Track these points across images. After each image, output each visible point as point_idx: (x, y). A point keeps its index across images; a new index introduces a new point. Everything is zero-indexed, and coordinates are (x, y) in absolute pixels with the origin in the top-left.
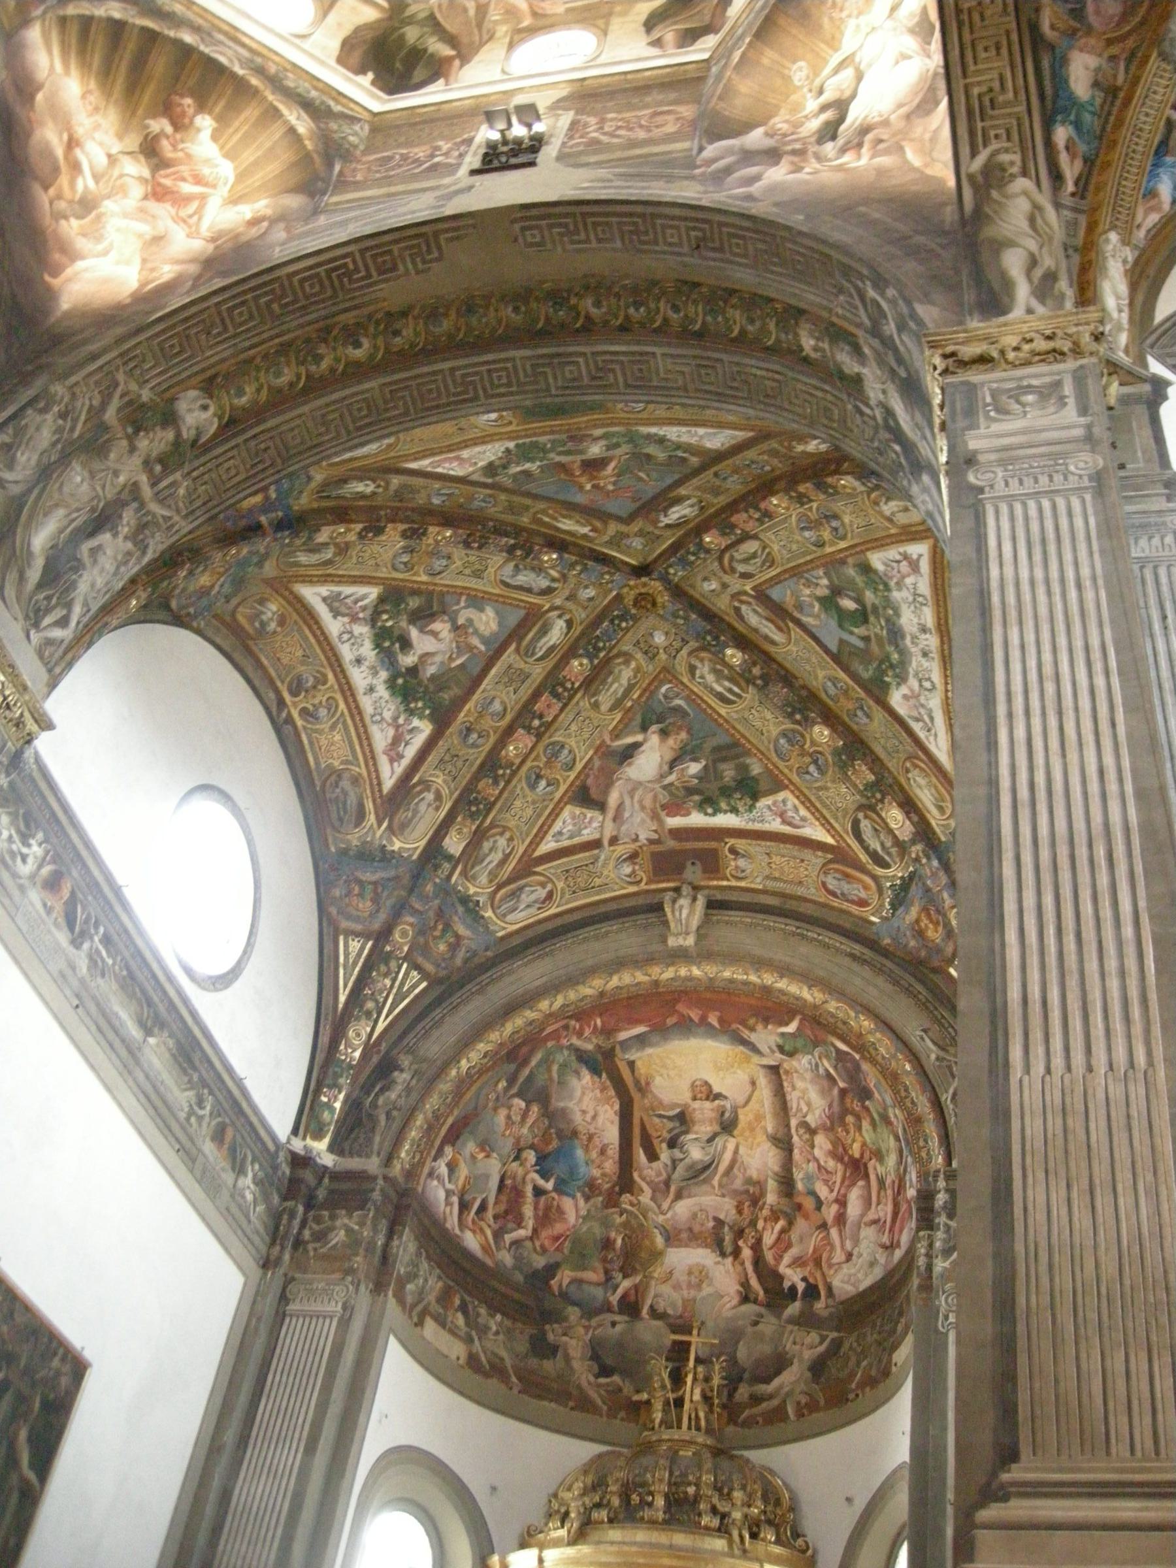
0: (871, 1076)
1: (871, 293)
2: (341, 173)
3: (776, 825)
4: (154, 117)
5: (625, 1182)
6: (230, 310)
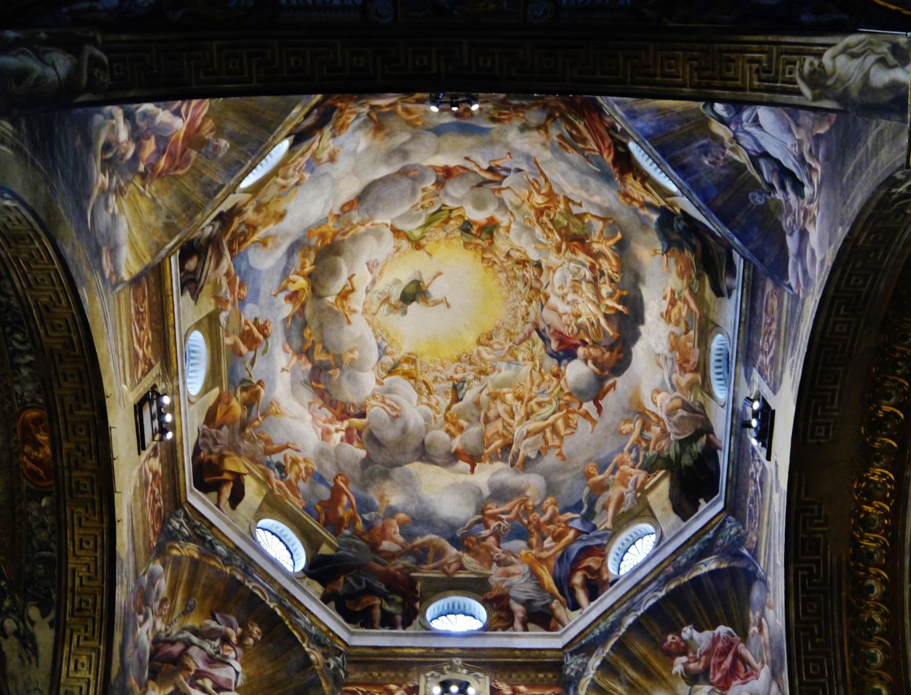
1: (902, 189)
2: (749, 550)
4: (672, 666)
6: (808, 675)
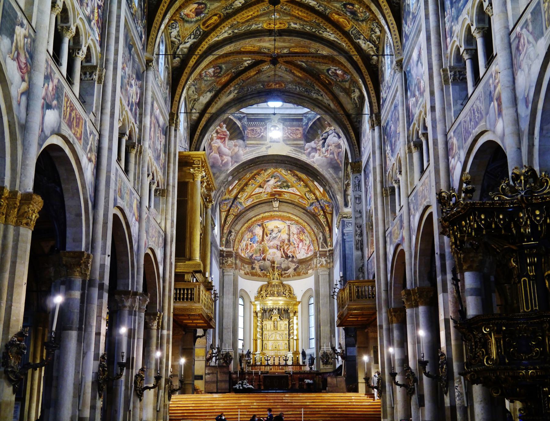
0: (306, 232)
3: (292, 192)
5: (263, 240)
